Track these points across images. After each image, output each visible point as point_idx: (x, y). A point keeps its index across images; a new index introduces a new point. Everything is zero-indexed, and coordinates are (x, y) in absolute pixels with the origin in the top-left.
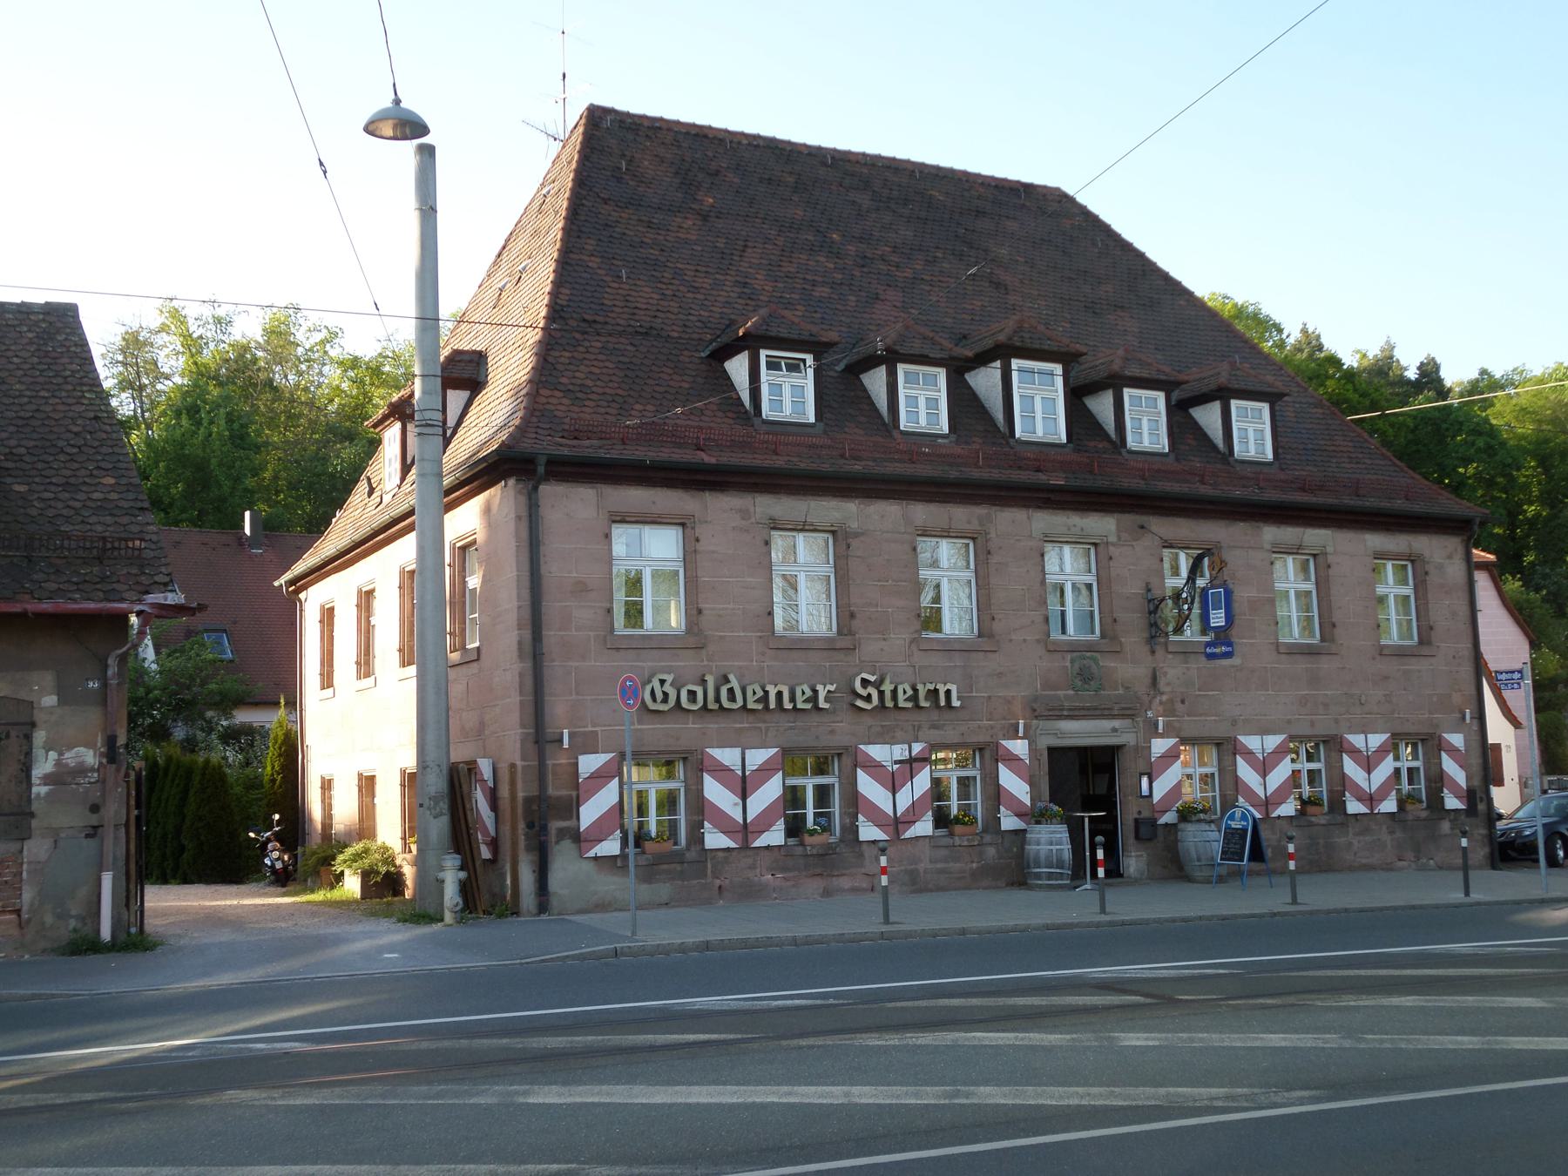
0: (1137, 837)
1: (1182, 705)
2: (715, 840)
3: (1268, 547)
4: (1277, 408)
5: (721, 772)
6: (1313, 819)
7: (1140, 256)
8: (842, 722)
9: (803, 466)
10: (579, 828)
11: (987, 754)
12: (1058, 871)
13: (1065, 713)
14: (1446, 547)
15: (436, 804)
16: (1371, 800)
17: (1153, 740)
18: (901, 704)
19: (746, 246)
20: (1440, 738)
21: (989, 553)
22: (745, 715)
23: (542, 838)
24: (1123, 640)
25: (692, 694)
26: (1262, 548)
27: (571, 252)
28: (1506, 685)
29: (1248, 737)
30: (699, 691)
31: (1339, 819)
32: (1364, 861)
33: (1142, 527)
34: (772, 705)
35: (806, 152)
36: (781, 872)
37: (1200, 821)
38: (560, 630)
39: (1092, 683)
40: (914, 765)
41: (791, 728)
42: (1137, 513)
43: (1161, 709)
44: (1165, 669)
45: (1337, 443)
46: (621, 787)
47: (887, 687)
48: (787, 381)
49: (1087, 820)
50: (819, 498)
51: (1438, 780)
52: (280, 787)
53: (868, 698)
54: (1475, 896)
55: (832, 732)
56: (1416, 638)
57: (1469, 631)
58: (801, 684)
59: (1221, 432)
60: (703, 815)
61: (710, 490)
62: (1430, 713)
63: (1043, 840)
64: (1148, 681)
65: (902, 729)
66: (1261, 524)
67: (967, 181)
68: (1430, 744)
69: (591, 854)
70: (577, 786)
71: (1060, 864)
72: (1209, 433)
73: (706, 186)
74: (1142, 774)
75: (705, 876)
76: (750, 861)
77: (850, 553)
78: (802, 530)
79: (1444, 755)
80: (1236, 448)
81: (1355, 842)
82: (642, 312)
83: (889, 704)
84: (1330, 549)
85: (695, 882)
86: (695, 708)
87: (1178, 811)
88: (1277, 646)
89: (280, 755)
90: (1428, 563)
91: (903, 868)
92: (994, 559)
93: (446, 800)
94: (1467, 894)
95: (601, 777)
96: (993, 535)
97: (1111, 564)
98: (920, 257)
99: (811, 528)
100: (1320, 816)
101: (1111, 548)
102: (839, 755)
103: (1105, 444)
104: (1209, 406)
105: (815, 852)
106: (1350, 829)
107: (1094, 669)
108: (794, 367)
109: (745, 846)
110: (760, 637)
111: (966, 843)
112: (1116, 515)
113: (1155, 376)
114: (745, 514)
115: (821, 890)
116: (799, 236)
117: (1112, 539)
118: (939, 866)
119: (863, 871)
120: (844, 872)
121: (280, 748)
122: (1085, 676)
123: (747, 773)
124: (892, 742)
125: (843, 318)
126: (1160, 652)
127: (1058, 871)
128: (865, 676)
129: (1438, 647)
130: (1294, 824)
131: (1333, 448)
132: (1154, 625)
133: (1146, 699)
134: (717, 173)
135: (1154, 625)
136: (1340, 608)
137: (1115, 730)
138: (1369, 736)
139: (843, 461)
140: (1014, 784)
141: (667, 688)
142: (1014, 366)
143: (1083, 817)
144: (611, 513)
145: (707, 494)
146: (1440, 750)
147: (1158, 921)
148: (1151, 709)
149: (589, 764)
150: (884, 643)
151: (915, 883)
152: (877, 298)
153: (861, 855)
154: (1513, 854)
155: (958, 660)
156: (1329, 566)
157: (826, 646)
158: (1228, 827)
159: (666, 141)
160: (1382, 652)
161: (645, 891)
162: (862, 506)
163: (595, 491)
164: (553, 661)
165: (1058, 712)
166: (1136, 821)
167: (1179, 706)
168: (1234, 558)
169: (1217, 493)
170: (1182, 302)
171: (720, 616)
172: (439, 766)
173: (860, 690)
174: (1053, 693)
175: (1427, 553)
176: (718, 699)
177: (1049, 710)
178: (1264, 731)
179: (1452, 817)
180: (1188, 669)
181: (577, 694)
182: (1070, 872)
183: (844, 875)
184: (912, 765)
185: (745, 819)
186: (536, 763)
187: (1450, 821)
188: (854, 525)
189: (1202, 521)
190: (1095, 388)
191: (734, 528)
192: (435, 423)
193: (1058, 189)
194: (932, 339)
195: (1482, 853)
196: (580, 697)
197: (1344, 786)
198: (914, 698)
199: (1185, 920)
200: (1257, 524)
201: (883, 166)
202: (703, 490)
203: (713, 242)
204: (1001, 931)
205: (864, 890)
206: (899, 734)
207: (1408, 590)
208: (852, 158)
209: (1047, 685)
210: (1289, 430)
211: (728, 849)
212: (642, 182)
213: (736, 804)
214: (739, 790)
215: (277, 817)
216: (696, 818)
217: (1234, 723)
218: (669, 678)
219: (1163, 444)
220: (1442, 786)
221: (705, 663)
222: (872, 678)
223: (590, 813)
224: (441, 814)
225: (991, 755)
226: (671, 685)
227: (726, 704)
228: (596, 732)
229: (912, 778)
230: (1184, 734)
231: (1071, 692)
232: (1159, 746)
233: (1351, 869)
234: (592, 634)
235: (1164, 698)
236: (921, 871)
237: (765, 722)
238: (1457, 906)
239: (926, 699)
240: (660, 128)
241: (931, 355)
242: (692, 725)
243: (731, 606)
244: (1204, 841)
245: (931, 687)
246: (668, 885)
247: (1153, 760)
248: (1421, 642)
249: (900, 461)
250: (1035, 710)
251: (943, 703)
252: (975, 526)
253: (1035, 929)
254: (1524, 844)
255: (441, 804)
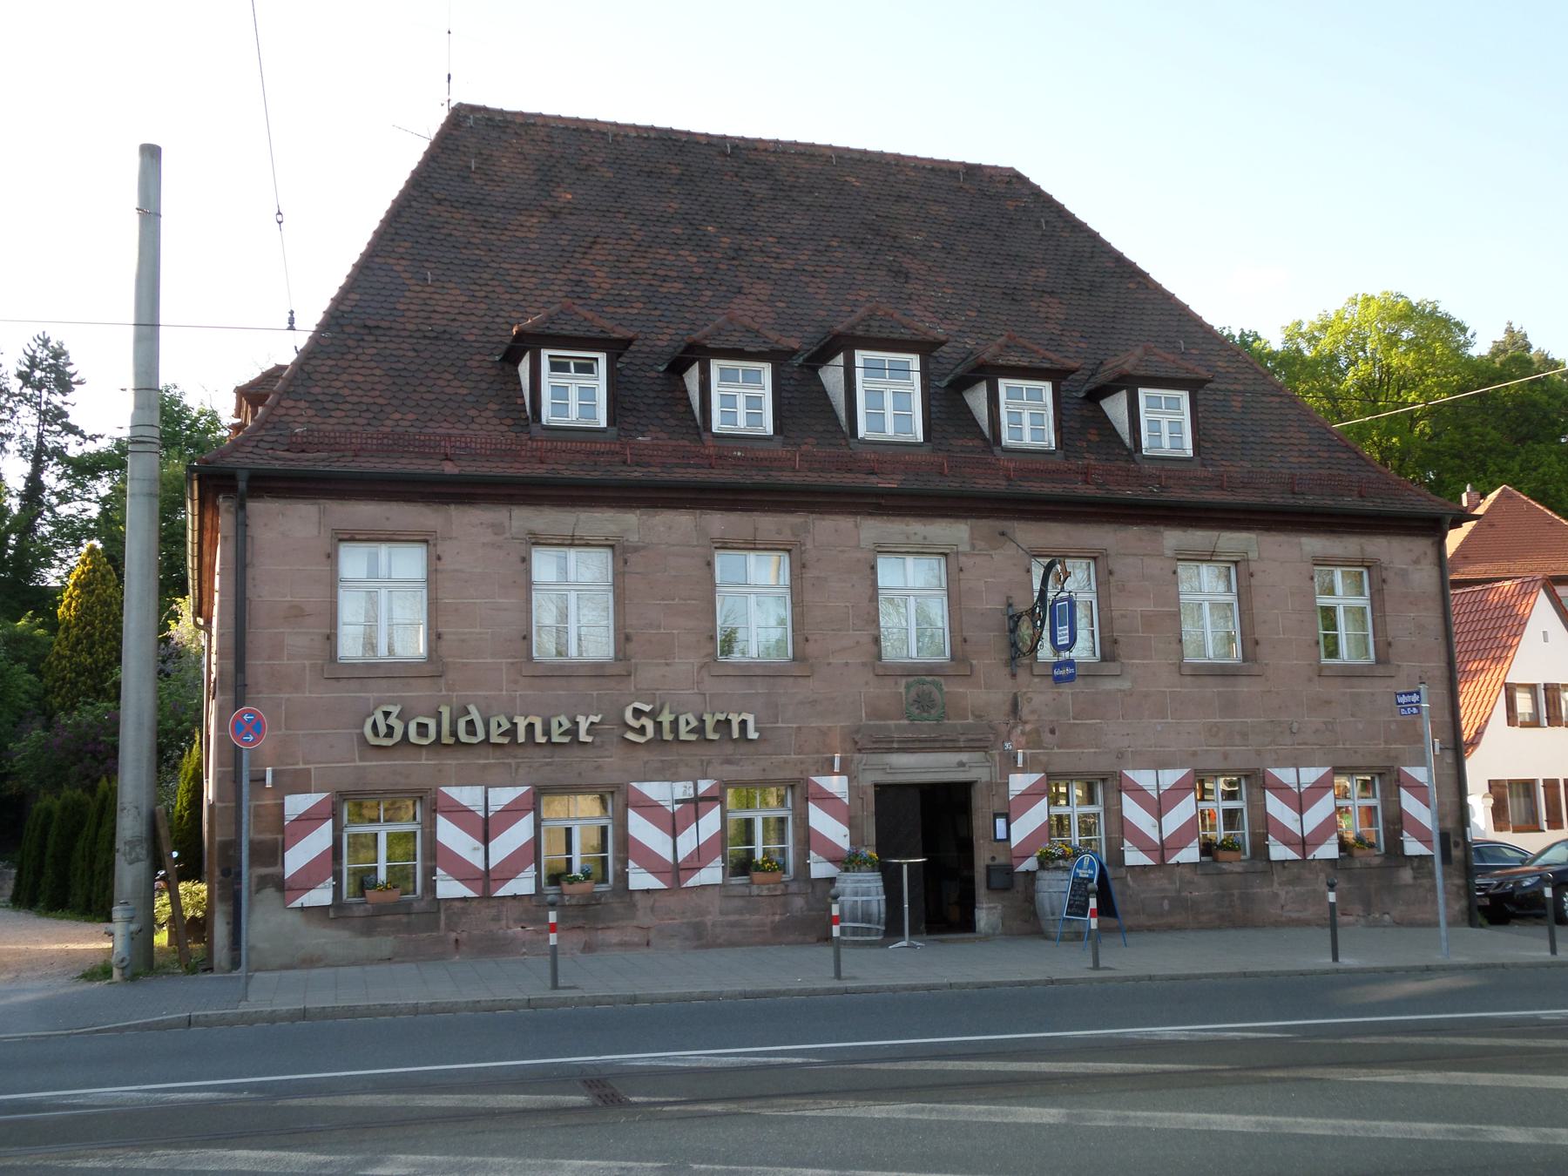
0: (988, 887)
1: (1049, 735)
2: (449, 888)
3: (1169, 553)
4: (1199, 397)
5: (459, 814)
6: (1225, 866)
7: (1094, 236)
8: (611, 757)
9: (567, 474)
10: (284, 876)
11: (798, 791)
12: (864, 925)
13: (895, 745)
14: (1411, 550)
15: (133, 848)
16: (1303, 844)
17: (1011, 776)
18: (683, 736)
19: (594, 243)
20: (1399, 771)
21: (804, 566)
22: (491, 750)
23: (236, 887)
24: (974, 662)
25: (422, 728)
26: (1163, 555)
27: (377, 256)
28: (1406, 709)
29: (1136, 772)
30: (432, 724)
31: (1260, 865)
32: (1294, 915)
33: (1003, 534)
34: (521, 738)
35: (704, 142)
36: (532, 925)
37: (1058, 868)
38: (270, 658)
39: (933, 711)
40: (700, 804)
41: (548, 764)
42: (998, 518)
43: (1023, 740)
44: (1029, 695)
45: (1288, 435)
46: (537, 827)
47: (666, 718)
48: (574, 382)
49: (905, 867)
50: (592, 510)
51: (1396, 822)
52: (187, 823)
53: (642, 730)
54: (1346, 961)
55: (599, 768)
56: (1372, 656)
57: (1442, 650)
58: (685, 713)
59: (1127, 425)
60: (436, 860)
61: (456, 503)
62: (1386, 742)
63: (848, 891)
64: (1007, 707)
65: (687, 765)
66: (1162, 528)
67: (896, 165)
68: (1387, 778)
69: (297, 903)
70: (282, 829)
71: (867, 918)
72: (1117, 427)
73: (568, 181)
74: (996, 816)
75: (438, 928)
76: (494, 912)
77: (439, 567)
78: (571, 545)
79: (1403, 792)
80: (1145, 443)
81: (1282, 894)
82: (439, 316)
83: (668, 736)
84: (1253, 555)
85: (425, 935)
86: (474, 740)
87: (1039, 858)
88: (1180, 667)
89: (188, 791)
90: (1386, 569)
91: (685, 920)
92: (810, 574)
93: (145, 846)
94: (1335, 958)
95: (309, 820)
96: (809, 546)
97: (962, 576)
98: (810, 247)
99: (583, 542)
100: (1233, 864)
101: (962, 559)
102: (612, 793)
103: (978, 442)
104: (1116, 396)
105: (574, 902)
106: (1275, 878)
107: (936, 695)
108: (586, 368)
109: (486, 896)
110: (512, 664)
111: (765, 893)
112: (969, 522)
113: (1037, 363)
114: (497, 529)
115: (582, 946)
116: (665, 230)
117: (965, 548)
118: (733, 918)
119: (635, 923)
120: (611, 925)
121: (189, 784)
122: (924, 703)
123: (490, 814)
124: (674, 779)
125: (687, 315)
126: (1023, 675)
127: (864, 925)
128: (638, 705)
129: (1399, 666)
130: (1199, 872)
131: (1282, 440)
132: (1014, 645)
133: (1004, 729)
134: (587, 168)
135: (1014, 645)
136: (1265, 622)
137: (961, 764)
138: (1160, 771)
139: (624, 468)
140: (829, 827)
141: (392, 721)
142: (859, 361)
143: (901, 865)
144: (336, 532)
145: (453, 507)
146: (1399, 786)
147: (893, 989)
148: (1009, 740)
149: (296, 805)
150: (667, 668)
151: (700, 938)
152: (739, 292)
153: (633, 906)
154: (1511, 908)
155: (761, 688)
156: (1252, 575)
157: (596, 672)
158: (1076, 876)
159: (536, 138)
160: (1185, 672)
161: (363, 945)
162: (644, 517)
163: (317, 506)
164: (259, 693)
165: (885, 745)
166: (988, 867)
167: (1047, 737)
168: (1125, 568)
169: (1101, 493)
170: (1131, 285)
171: (463, 641)
172: (137, 808)
173: (630, 719)
174: (882, 723)
175: (1384, 559)
176: (454, 733)
177: (874, 742)
178: (1159, 764)
179: (1415, 864)
180: (1060, 694)
181: (286, 729)
182: (883, 928)
183: (609, 928)
184: (697, 805)
185: (487, 865)
186: (233, 804)
187: (1413, 869)
188: (634, 538)
189: (1082, 525)
190: (964, 383)
191: (484, 544)
192: (154, 440)
193: (1012, 169)
194: (758, 331)
195: (1457, 907)
196: (291, 732)
197: (1267, 829)
198: (700, 730)
199: (929, 988)
200: (1157, 528)
201: (796, 153)
202: (447, 504)
203: (555, 240)
204: (686, 999)
205: (638, 945)
206: (683, 770)
207: (1363, 602)
208: (760, 146)
209: (875, 713)
210: (1229, 422)
211: (465, 899)
212: (492, 180)
213: (475, 849)
214: (670, 830)
215: (175, 854)
216: (429, 864)
217: (1120, 755)
218: (395, 710)
219: (1049, 440)
220: (1402, 828)
221: (444, 693)
222: (647, 708)
223: (296, 858)
224: (138, 860)
225: (802, 792)
226: (397, 717)
227: (464, 738)
228: (309, 771)
229: (697, 819)
230: (1052, 769)
231: (906, 722)
232: (1019, 782)
233: (1278, 924)
234: (307, 663)
235: (1028, 727)
236: (709, 924)
237: (515, 757)
238: (1326, 972)
239: (715, 730)
240: (534, 125)
241: (747, 349)
242: (425, 761)
243: (477, 630)
244: (1054, 889)
245: (722, 717)
246: (391, 938)
247: (286, 823)
248: (1378, 661)
249: (698, 466)
250: (856, 743)
251: (736, 735)
252: (787, 535)
253: (727, 997)
254: (1524, 896)
255: (138, 849)
